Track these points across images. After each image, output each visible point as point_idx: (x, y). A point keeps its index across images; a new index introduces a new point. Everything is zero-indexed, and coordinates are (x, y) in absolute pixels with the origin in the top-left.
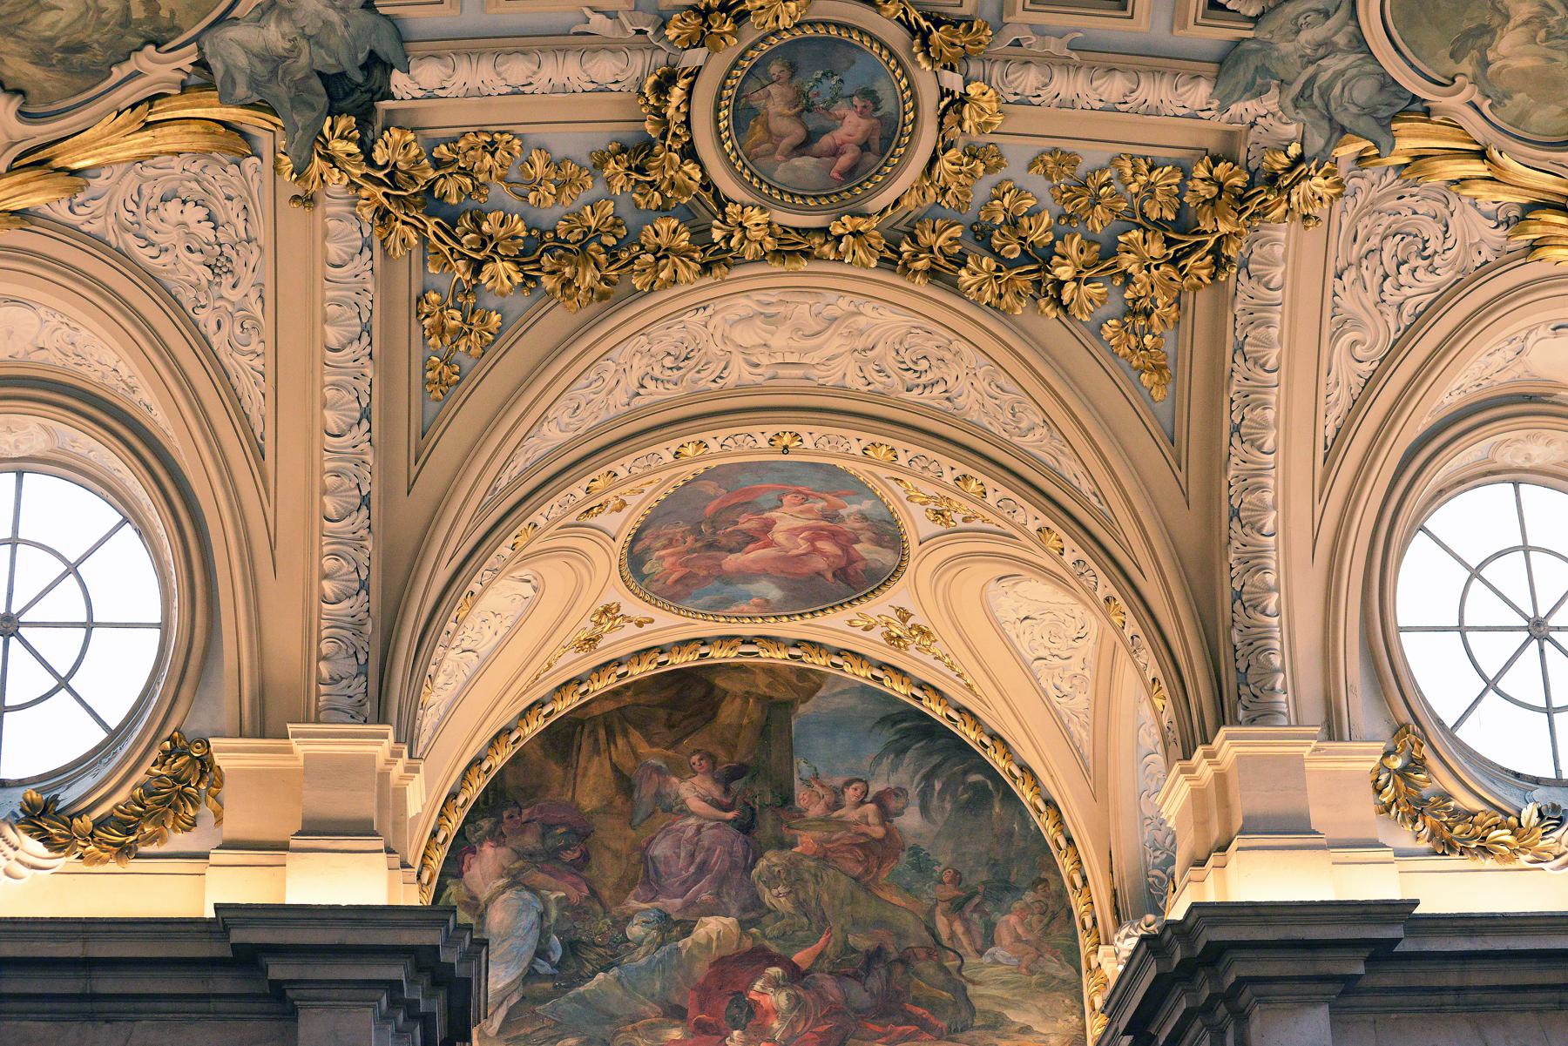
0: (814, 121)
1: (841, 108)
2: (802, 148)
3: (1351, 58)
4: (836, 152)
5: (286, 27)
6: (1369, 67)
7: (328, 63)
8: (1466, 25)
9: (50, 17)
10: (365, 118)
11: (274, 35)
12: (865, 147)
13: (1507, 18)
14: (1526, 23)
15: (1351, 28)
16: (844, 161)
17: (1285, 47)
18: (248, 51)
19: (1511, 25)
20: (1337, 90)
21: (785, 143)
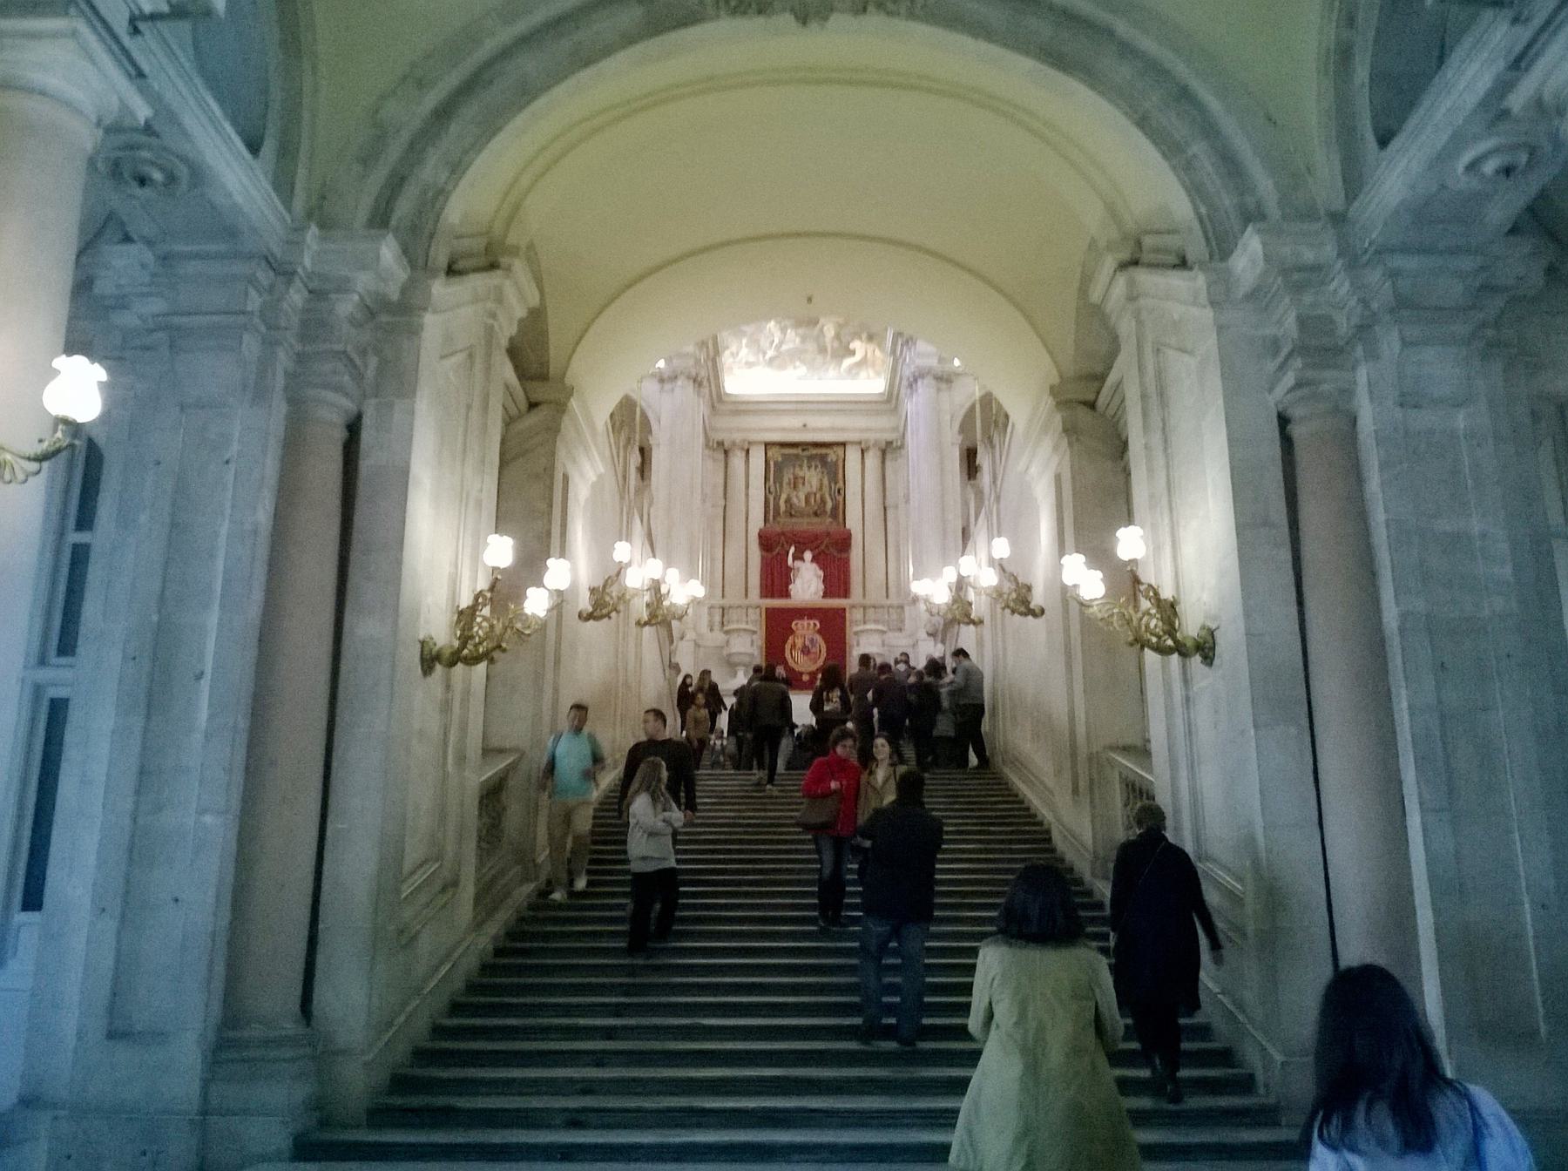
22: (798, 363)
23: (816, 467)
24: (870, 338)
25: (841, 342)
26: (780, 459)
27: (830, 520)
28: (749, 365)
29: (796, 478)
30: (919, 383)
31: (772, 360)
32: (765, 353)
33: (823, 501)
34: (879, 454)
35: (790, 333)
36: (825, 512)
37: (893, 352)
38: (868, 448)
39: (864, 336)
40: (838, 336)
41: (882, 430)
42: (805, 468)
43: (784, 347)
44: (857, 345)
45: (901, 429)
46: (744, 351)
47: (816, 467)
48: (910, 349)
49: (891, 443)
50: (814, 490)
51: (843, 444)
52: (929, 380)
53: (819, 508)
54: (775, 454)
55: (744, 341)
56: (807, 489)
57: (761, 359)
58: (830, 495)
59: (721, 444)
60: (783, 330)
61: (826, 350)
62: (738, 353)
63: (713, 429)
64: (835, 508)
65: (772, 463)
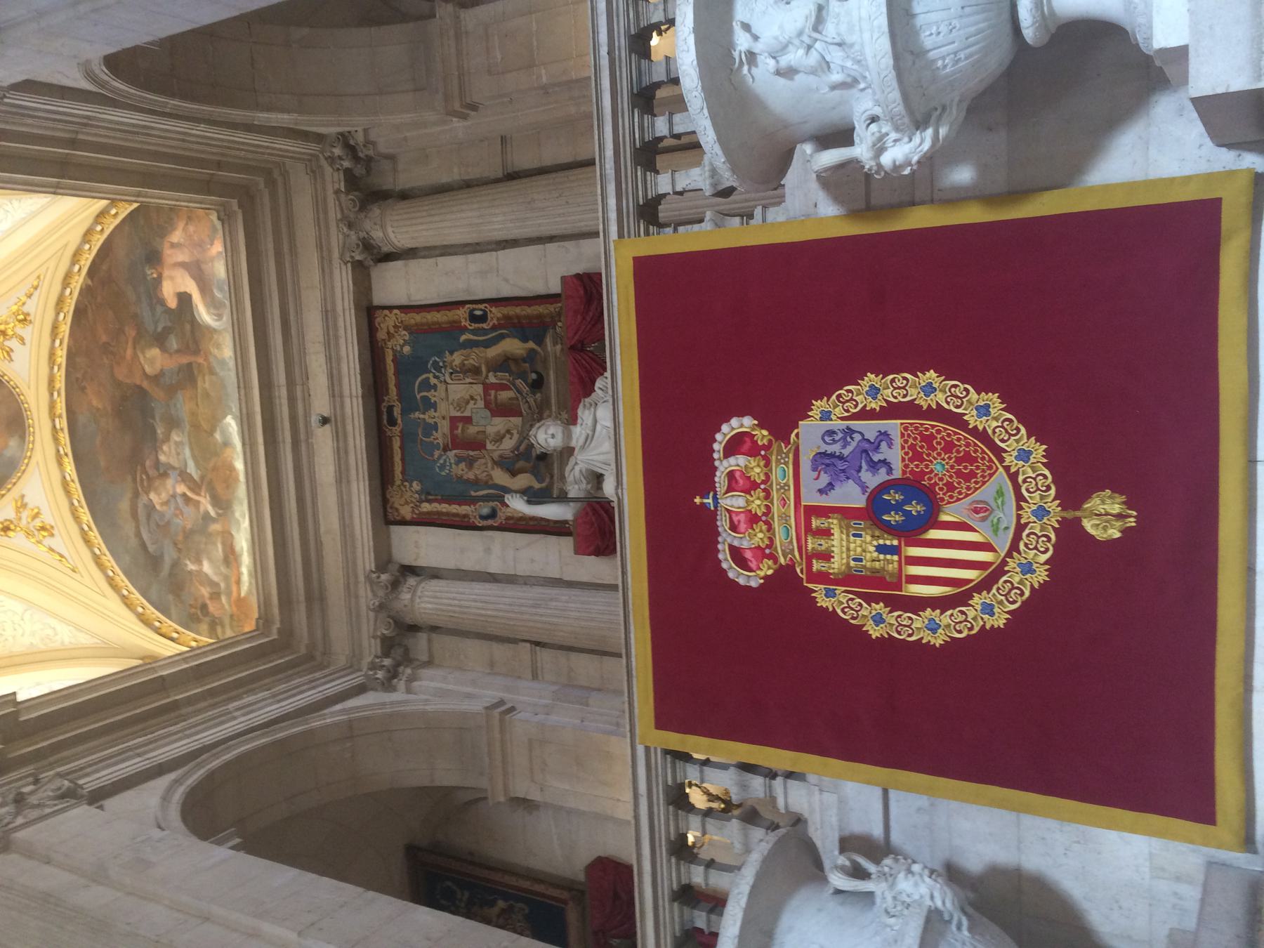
22: (218, 436)
23: (426, 386)
24: (154, 258)
25: (167, 331)
26: (416, 486)
27: (548, 341)
29: (456, 442)
31: (216, 501)
32: (206, 517)
33: (504, 364)
34: (376, 211)
35: (167, 455)
36: (531, 355)
38: (367, 245)
39: (152, 273)
40: (160, 340)
41: (320, 206)
42: (428, 417)
43: (192, 469)
45: (313, 148)
46: (207, 567)
47: (426, 386)
49: (348, 172)
50: (479, 389)
51: (369, 313)
53: (523, 375)
54: (405, 500)
55: (191, 567)
56: (477, 409)
58: (487, 344)
59: (388, 645)
61: (190, 365)
62: (214, 584)
63: (351, 667)
64: (521, 328)
65: (426, 507)
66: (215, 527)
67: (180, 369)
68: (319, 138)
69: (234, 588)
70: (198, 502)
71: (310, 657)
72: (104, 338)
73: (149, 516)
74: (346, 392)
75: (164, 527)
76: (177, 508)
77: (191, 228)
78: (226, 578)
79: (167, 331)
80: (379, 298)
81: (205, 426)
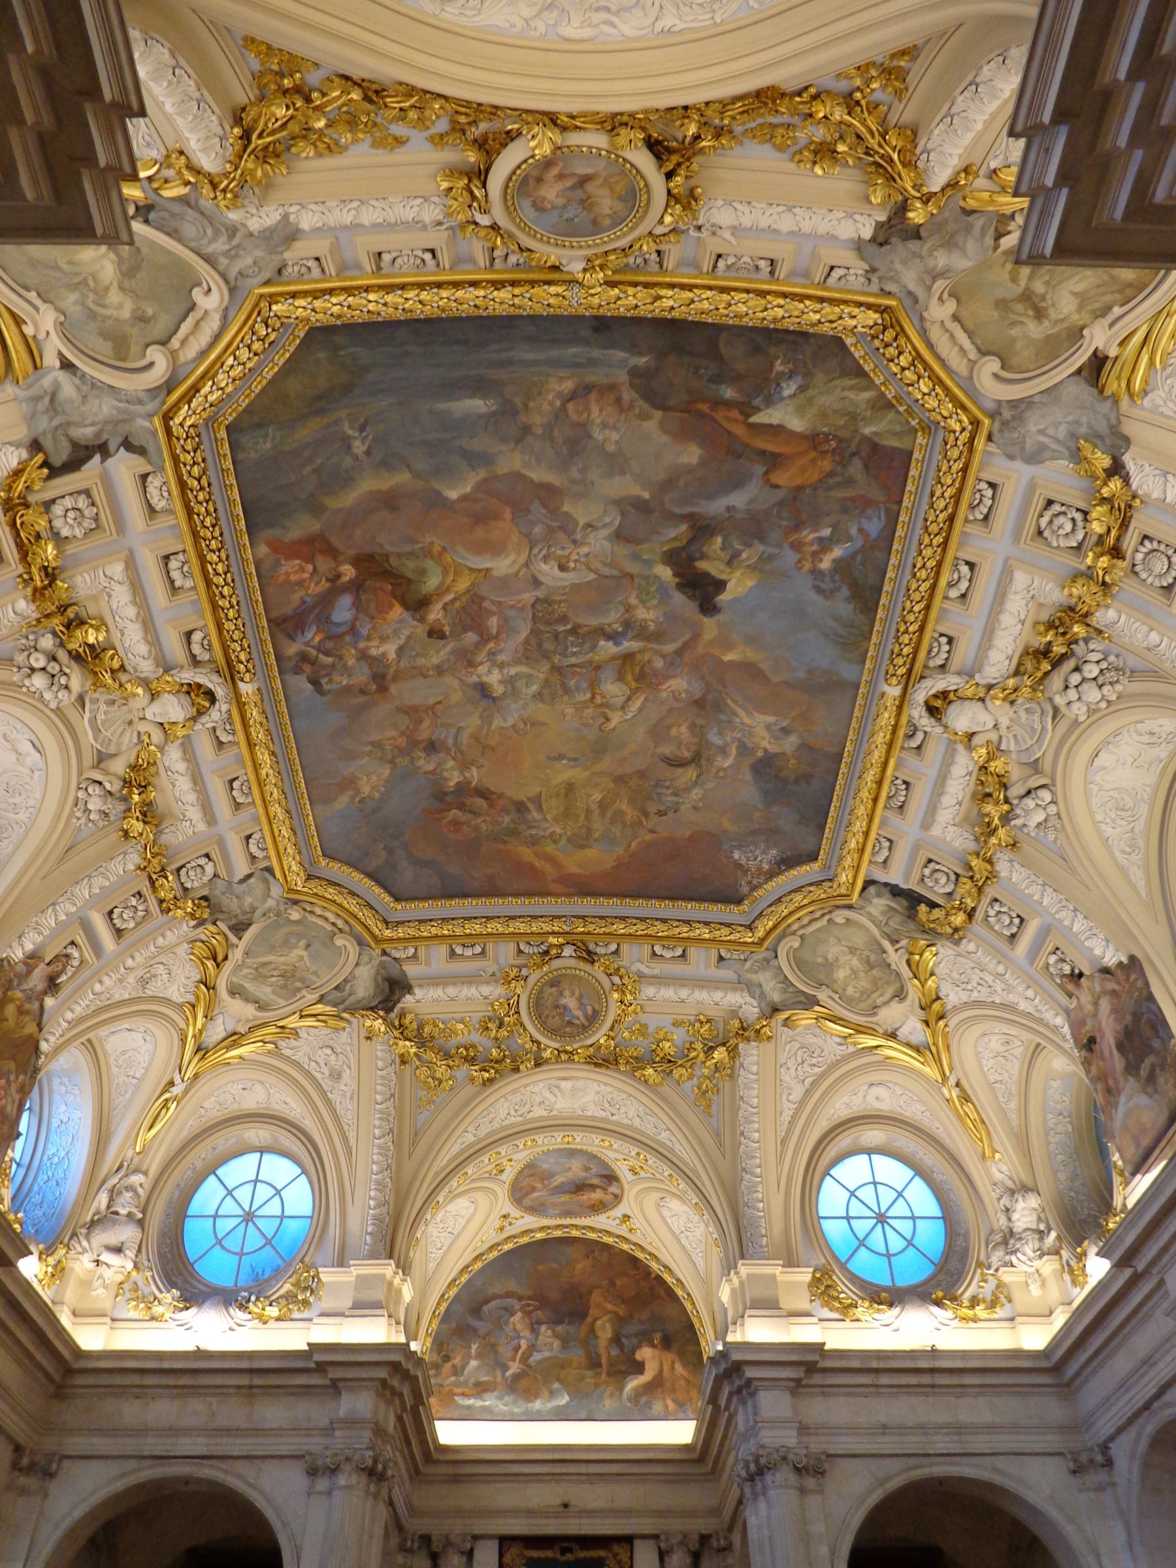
0: (579, 193)
1: (560, 201)
2: (584, 180)
3: (210, 249)
4: (561, 177)
5: (931, 263)
6: (193, 244)
7: (913, 245)
8: (142, 274)
9: (1080, 287)
10: (902, 208)
11: (942, 259)
12: (539, 180)
13: (122, 288)
14: (107, 289)
15: (221, 268)
16: (555, 171)
17: (258, 253)
18: (964, 251)
19: (115, 284)
20: (209, 231)
21: (599, 181)
22: (556, 1385)
24: (667, 1343)
28: (481, 1389)
30: (768, 1478)
31: (517, 1377)
32: (505, 1368)
37: (713, 1400)
40: (616, 1340)
43: (537, 1357)
44: (646, 1354)
46: (474, 1363)
48: (744, 1403)
52: (783, 1476)
55: (474, 1347)
57: (499, 1379)
60: (533, 1330)
61: (599, 1365)
62: (463, 1368)
63: (413, 1511)
66: (499, 1373)
67: (598, 1355)
68: (730, 1528)
69: (458, 1390)
70: (514, 1360)
71: (417, 1471)
72: (618, 1283)
73: (506, 1309)
74: (584, 1521)
75: (499, 1324)
76: (513, 1339)
77: (683, 1382)
78: (466, 1383)
79: (621, 1346)
80: (637, 1543)
81: (563, 1374)
